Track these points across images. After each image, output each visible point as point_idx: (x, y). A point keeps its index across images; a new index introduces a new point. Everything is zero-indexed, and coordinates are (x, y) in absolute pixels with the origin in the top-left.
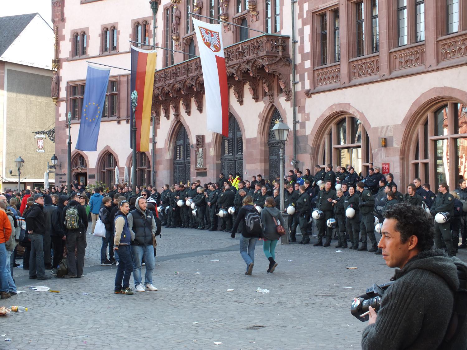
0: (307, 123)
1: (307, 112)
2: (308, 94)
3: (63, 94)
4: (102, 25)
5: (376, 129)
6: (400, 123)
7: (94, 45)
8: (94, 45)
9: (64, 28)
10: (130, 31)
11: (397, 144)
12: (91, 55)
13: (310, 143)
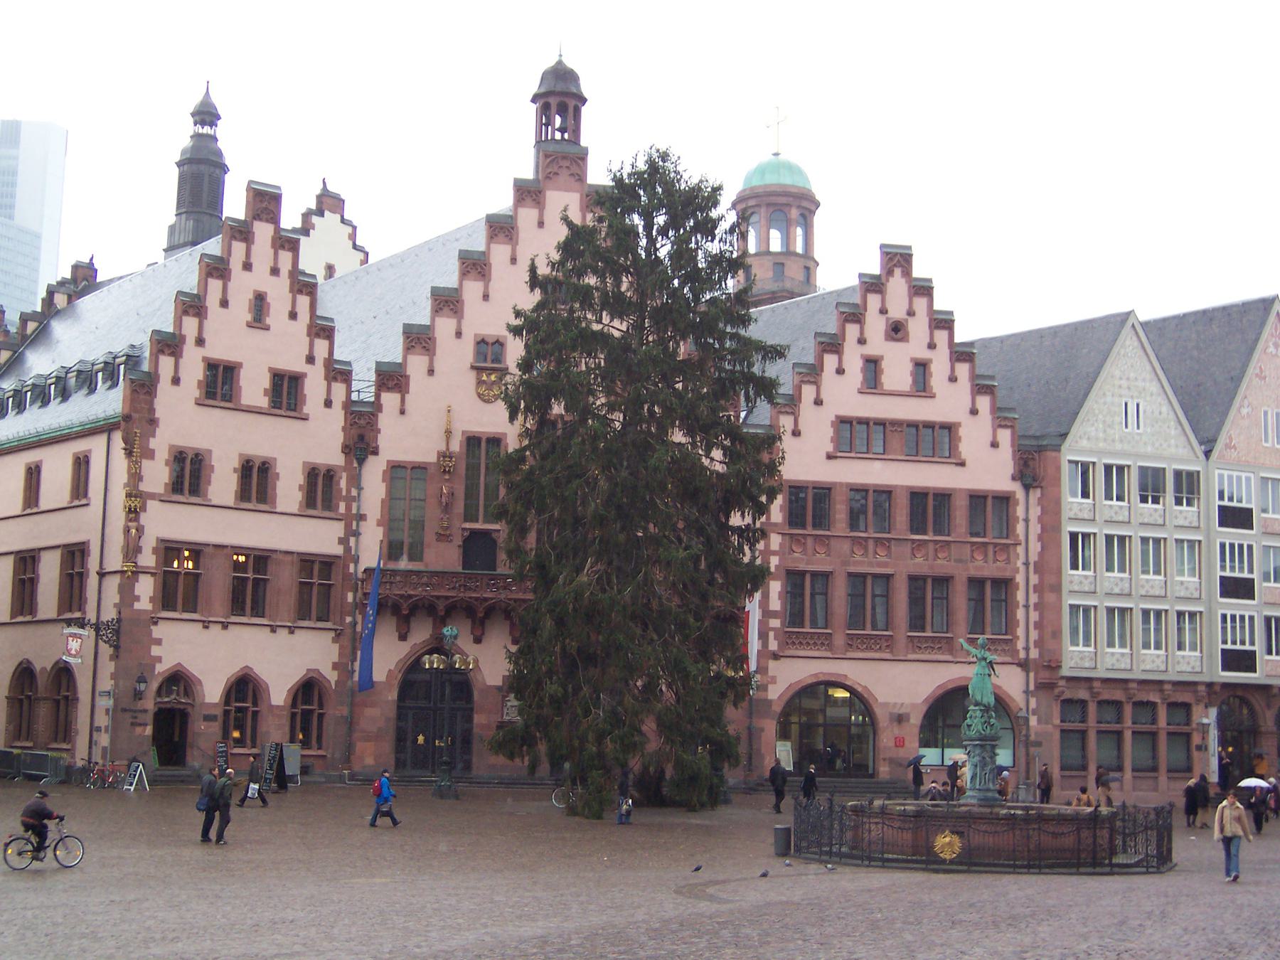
0: (770, 687)
1: (770, 673)
2: (776, 656)
3: (148, 559)
4: (241, 455)
5: (886, 705)
6: (920, 701)
7: (223, 484)
8: (223, 484)
9: (154, 436)
10: (300, 479)
11: (916, 720)
12: (214, 502)
13: (777, 708)
